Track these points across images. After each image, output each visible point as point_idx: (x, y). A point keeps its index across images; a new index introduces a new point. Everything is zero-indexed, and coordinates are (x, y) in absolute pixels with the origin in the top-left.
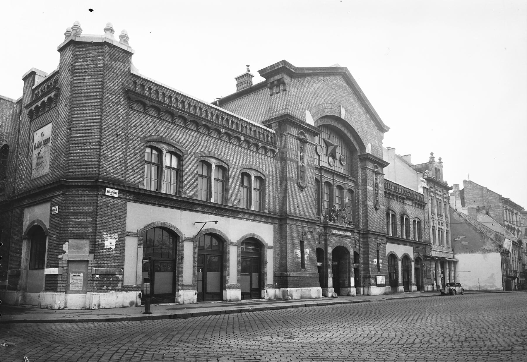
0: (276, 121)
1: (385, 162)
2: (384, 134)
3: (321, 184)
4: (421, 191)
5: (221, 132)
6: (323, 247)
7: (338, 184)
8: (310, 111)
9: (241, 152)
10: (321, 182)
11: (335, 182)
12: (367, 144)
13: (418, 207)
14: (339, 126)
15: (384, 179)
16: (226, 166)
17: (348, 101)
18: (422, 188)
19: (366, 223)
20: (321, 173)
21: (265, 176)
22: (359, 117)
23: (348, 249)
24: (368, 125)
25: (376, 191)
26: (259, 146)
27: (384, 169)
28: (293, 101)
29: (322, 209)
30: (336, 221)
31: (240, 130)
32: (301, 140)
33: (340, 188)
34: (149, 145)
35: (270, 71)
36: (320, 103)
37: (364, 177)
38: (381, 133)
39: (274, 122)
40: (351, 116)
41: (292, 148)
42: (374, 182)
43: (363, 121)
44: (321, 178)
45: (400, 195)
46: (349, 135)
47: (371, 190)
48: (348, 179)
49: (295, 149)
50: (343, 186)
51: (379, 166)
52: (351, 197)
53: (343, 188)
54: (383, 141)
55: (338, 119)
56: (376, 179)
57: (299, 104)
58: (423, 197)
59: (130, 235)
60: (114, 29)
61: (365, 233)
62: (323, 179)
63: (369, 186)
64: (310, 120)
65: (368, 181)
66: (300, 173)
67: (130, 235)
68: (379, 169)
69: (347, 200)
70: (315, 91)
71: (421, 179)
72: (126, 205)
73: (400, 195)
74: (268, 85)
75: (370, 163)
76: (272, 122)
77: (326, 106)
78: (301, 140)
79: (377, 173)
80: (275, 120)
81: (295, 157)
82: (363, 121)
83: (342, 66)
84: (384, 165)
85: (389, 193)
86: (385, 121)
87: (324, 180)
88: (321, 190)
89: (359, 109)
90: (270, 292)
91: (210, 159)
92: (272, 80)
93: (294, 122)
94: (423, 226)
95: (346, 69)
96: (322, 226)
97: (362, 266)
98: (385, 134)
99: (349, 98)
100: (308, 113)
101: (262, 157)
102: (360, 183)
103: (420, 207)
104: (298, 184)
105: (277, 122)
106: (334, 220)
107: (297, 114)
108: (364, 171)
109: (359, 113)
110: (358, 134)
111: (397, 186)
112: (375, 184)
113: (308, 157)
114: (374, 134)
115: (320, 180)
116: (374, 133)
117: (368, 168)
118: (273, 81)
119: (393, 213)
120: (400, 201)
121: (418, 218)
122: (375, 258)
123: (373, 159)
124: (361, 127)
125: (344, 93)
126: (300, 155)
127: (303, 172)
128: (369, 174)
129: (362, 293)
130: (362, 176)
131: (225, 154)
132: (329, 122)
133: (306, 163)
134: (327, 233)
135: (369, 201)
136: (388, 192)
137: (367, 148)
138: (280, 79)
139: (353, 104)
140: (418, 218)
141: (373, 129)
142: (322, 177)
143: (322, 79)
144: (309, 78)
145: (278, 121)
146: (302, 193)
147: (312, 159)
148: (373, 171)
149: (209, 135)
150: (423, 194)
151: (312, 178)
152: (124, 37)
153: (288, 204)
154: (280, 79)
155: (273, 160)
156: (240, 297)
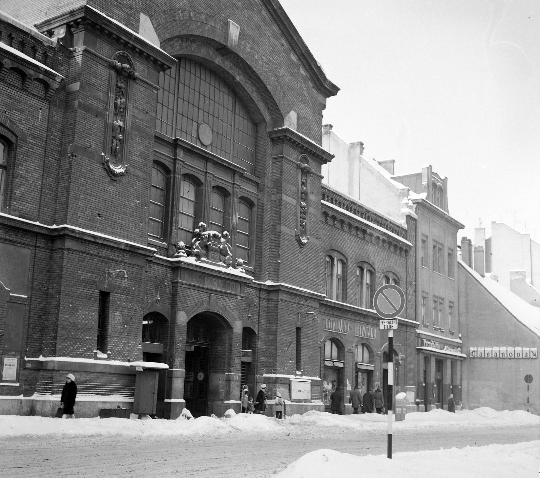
0: (62, 23)
1: (324, 152)
3: (174, 177)
6: (163, 309)
8: (151, 17)
10: (174, 174)
11: (208, 178)
12: (289, 112)
13: (395, 253)
14: (227, 65)
15: (323, 187)
17: (248, 18)
20: (175, 155)
21: (16, 136)
25: (301, 207)
26: (3, 64)
27: (324, 166)
29: (171, 230)
32: (119, 72)
36: (178, 6)
37: (278, 175)
38: (320, 98)
39: (58, 24)
41: (93, 85)
42: (298, 188)
44: (175, 163)
47: (292, 205)
48: (242, 176)
49: (105, 90)
50: (229, 189)
51: (311, 158)
52: (248, 215)
53: (230, 194)
54: (324, 112)
56: (303, 183)
58: (406, 234)
63: (286, 195)
65: (284, 185)
68: (311, 165)
69: (235, 219)
75: (292, 151)
78: (119, 72)
79: (306, 172)
81: (101, 106)
84: (322, 158)
85: (332, 216)
87: (181, 169)
98: (330, 101)
99: (250, 12)
100: (145, 21)
101: (14, 92)
104: (103, 164)
105: (64, 24)
108: (278, 163)
109: (273, 48)
112: (302, 193)
113: (136, 111)
115: (171, 167)
117: (286, 159)
119: (342, 257)
120: (357, 236)
121: (394, 273)
123: (299, 144)
124: (276, 76)
126: (116, 104)
128: (289, 169)
132: (201, 52)
133: (129, 123)
135: (285, 226)
137: (286, 119)
139: (258, 27)
140: (394, 273)
145: (65, 22)
146: (114, 186)
147: (147, 117)
148: (298, 167)
151: (146, 158)
155: (45, 105)
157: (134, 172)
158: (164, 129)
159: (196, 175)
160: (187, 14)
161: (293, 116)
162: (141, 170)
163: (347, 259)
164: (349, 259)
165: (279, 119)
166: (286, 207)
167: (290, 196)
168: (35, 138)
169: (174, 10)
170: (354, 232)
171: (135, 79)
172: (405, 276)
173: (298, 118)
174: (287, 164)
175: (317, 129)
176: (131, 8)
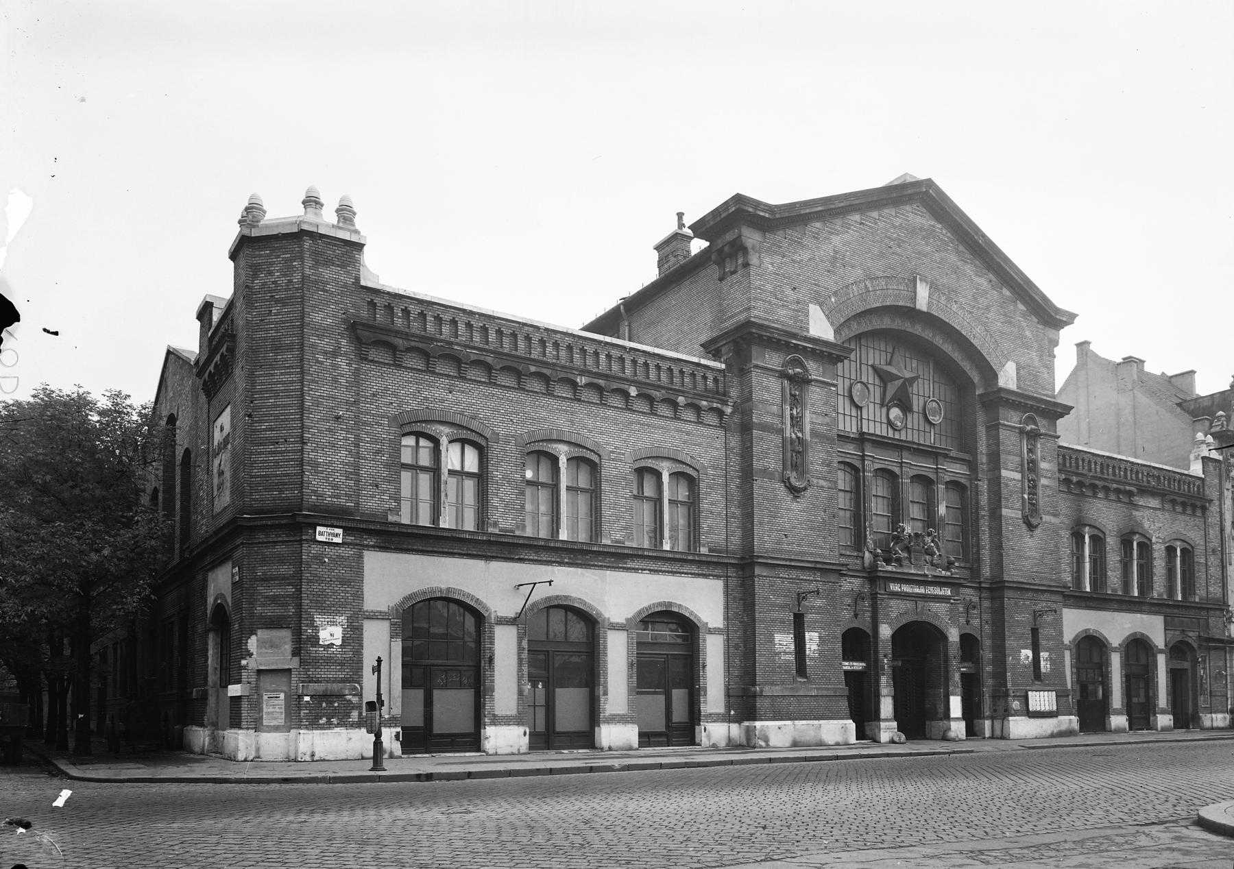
0: (728, 340)
2: (1062, 331)
3: (864, 476)
4: (1196, 469)
5: (577, 383)
7: (916, 472)
9: (631, 423)
10: (864, 472)
11: (904, 469)
13: (1184, 513)
16: (595, 458)
18: (1200, 461)
19: (998, 564)
20: (863, 451)
21: (698, 471)
22: (976, 299)
23: (943, 628)
24: (1006, 315)
25: (1029, 481)
26: (678, 403)
27: (1060, 422)
28: (769, 287)
29: (866, 535)
30: (906, 562)
31: (628, 371)
32: (791, 379)
33: (923, 481)
34: (408, 429)
35: (712, 223)
37: (994, 447)
39: (724, 342)
40: (949, 299)
41: (767, 400)
42: (1022, 459)
43: (988, 308)
44: (863, 460)
45: (1115, 486)
46: (948, 348)
47: (1014, 480)
48: (946, 456)
49: (778, 401)
50: (932, 476)
51: (1040, 416)
52: (959, 502)
53: (933, 481)
55: (911, 313)
56: (1030, 451)
57: (789, 292)
58: (1203, 484)
59: (374, 616)
60: (322, 200)
61: (996, 589)
62: (870, 462)
64: (820, 327)
65: (1003, 457)
66: (792, 456)
67: (374, 616)
69: (942, 510)
70: (836, 252)
71: (1200, 436)
72: (361, 557)
73: (1115, 486)
74: (713, 257)
75: (1012, 413)
76: (721, 344)
77: (869, 285)
78: (791, 379)
80: (725, 339)
81: (776, 421)
82: (988, 308)
83: (922, 176)
84: (1056, 412)
85: (1077, 482)
86: (1059, 298)
88: (864, 490)
89: (977, 279)
90: (715, 732)
91: (554, 446)
92: (720, 243)
93: (770, 339)
94: (1203, 561)
95: (929, 183)
96: (863, 577)
97: (989, 669)
100: (815, 312)
101: (690, 427)
102: (982, 464)
103: (1189, 512)
104: (785, 482)
106: (899, 560)
107: (781, 317)
108: (994, 432)
110: (974, 342)
111: (1108, 461)
112: (1028, 463)
113: (814, 416)
114: (1026, 337)
115: (860, 467)
116: (1028, 333)
117: (1004, 425)
118: (721, 246)
120: (1119, 501)
121: (1184, 541)
122: (1026, 648)
123: (1020, 402)
125: (927, 244)
126: (791, 414)
127: (799, 452)
128: (1008, 439)
129: (987, 734)
130: (988, 446)
131: (590, 431)
134: (877, 593)
136: (1075, 479)
138: (735, 240)
140: (1184, 541)
141: (1024, 324)
142: (866, 458)
143: (859, 220)
144: (818, 225)
145: (731, 339)
146: (798, 502)
147: (827, 420)
148: (1022, 432)
149: (549, 394)
150: (1203, 476)
152: (345, 213)
153: (757, 530)
154: (736, 239)
155: (721, 433)
156: (635, 741)
157: (818, 483)
158: (848, 424)
159: (889, 468)
160: (862, 285)
161: (1010, 368)
162: (824, 479)
163: (1104, 534)
164: (1107, 533)
165: (990, 375)
166: (1007, 485)
167: (1013, 470)
168: (715, 468)
169: (847, 287)
170: (1113, 496)
171: (809, 382)
172: (1202, 543)
173: (1018, 370)
174: (1003, 431)
175: (1046, 376)
176: (798, 303)
